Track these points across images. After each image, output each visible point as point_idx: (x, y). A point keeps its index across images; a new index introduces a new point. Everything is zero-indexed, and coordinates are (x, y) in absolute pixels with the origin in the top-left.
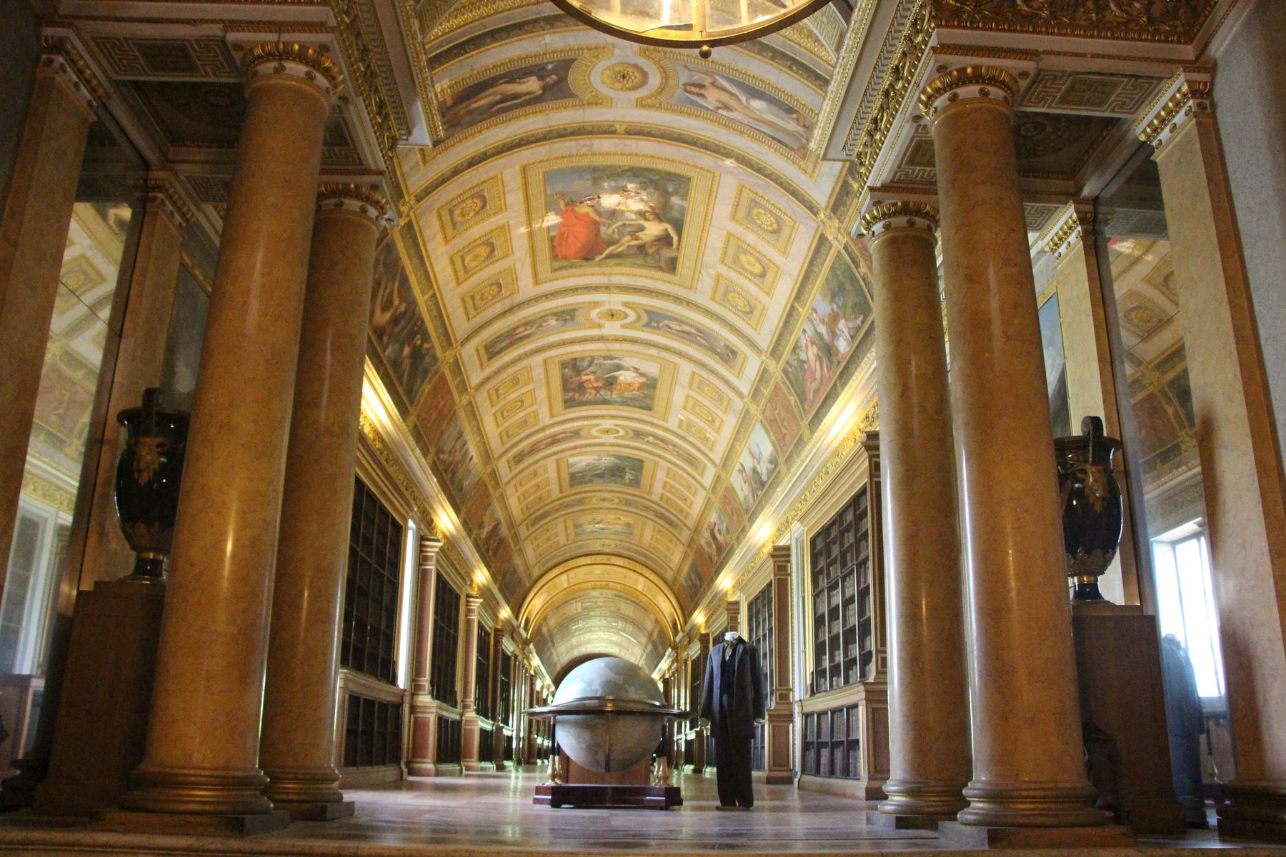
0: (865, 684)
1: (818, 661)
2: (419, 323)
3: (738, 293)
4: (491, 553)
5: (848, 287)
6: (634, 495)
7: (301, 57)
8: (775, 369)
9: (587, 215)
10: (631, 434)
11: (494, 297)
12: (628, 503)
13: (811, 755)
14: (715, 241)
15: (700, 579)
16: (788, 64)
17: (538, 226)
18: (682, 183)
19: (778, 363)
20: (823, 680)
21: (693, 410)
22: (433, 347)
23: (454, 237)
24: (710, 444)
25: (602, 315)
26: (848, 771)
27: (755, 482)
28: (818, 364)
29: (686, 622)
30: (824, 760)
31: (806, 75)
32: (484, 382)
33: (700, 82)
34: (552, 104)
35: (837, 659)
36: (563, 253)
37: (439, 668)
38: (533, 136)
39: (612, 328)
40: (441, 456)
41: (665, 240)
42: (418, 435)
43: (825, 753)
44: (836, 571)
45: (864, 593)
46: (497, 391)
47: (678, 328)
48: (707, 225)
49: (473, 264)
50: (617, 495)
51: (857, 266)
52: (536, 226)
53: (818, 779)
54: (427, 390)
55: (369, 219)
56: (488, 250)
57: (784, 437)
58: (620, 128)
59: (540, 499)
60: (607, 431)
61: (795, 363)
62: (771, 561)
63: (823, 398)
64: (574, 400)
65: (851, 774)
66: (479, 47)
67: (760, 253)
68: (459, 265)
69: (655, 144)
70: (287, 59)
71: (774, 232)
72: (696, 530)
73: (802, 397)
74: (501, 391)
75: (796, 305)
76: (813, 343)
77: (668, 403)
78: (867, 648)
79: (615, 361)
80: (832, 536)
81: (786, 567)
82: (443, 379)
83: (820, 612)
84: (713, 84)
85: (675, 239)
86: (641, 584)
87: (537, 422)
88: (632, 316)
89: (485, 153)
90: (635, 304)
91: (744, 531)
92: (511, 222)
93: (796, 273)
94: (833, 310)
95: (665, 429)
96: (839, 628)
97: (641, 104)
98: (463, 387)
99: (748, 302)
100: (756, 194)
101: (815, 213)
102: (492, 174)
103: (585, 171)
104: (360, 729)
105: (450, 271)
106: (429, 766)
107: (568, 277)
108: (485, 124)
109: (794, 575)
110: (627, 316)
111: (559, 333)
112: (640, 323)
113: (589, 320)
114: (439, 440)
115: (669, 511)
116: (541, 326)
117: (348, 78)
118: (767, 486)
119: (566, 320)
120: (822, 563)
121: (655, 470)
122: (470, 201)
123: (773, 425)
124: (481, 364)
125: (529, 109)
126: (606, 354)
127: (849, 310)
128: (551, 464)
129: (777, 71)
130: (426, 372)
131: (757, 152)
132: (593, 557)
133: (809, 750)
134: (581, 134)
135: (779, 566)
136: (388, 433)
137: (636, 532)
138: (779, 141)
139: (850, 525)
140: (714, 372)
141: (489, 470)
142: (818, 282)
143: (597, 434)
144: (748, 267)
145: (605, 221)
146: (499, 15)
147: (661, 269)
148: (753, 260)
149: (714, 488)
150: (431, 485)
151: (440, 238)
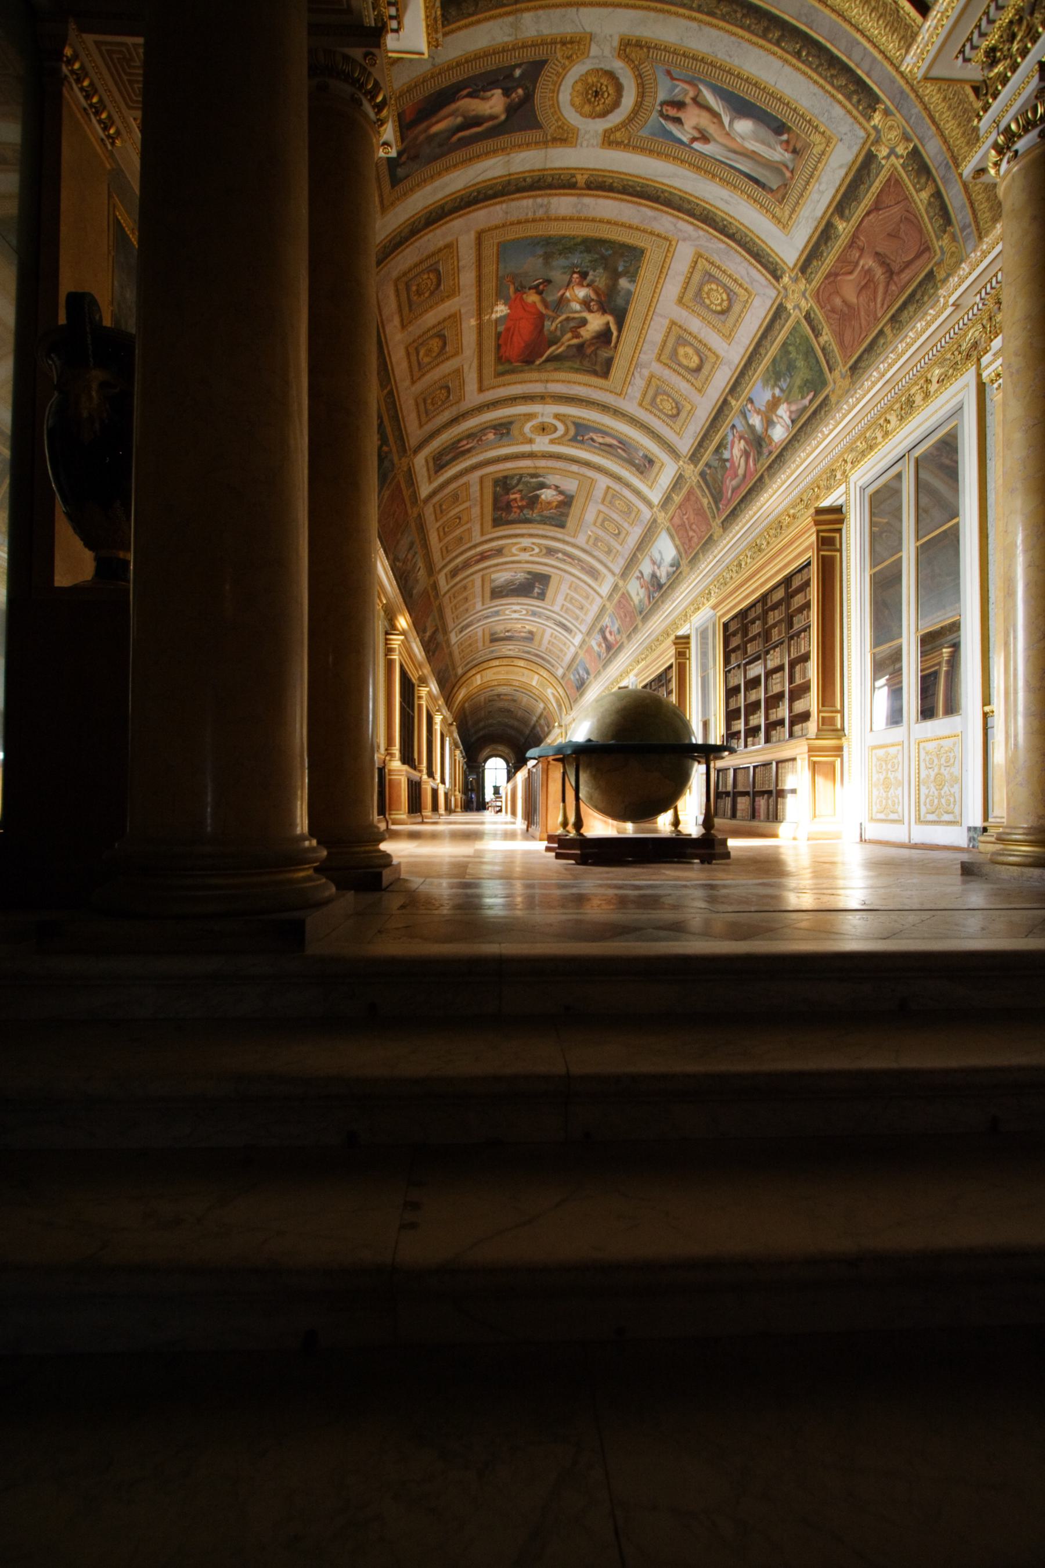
1: (728, 726)
3: (669, 396)
4: (431, 653)
5: (800, 363)
6: (538, 607)
8: (692, 473)
10: (544, 551)
11: (443, 403)
12: (534, 614)
14: (656, 333)
15: (588, 673)
17: (487, 317)
19: (696, 466)
22: (391, 451)
27: (653, 586)
33: (680, 98)
34: (518, 137)
36: (507, 354)
38: (491, 187)
39: (542, 444)
40: (397, 564)
41: (604, 337)
46: (441, 506)
47: (601, 440)
48: (651, 313)
49: (427, 360)
51: (817, 334)
53: (734, 822)
56: (440, 344)
57: (690, 541)
58: (581, 179)
60: (525, 550)
61: (716, 464)
62: (674, 647)
63: (743, 494)
67: (700, 341)
68: (414, 358)
73: (717, 497)
74: (444, 507)
75: (729, 398)
76: (741, 438)
77: (581, 519)
79: (541, 479)
80: (750, 618)
85: (615, 334)
86: (535, 681)
87: (470, 540)
89: (442, 207)
90: (564, 415)
91: (635, 629)
92: (463, 311)
95: (574, 546)
98: (415, 496)
99: (676, 404)
100: (712, 263)
101: (778, 279)
105: (405, 365)
107: (509, 384)
111: (494, 448)
113: (523, 434)
114: (395, 547)
115: (566, 619)
118: (664, 588)
119: (502, 434)
121: (560, 582)
122: (426, 276)
123: (680, 532)
124: (429, 478)
126: (532, 471)
127: (796, 389)
128: (477, 578)
131: (727, 202)
133: (722, 798)
134: (540, 189)
135: (679, 652)
137: (537, 638)
138: (756, 181)
140: (628, 485)
141: (431, 582)
142: (762, 366)
144: (685, 362)
145: (550, 313)
147: (595, 373)
149: (610, 597)
151: (396, 321)
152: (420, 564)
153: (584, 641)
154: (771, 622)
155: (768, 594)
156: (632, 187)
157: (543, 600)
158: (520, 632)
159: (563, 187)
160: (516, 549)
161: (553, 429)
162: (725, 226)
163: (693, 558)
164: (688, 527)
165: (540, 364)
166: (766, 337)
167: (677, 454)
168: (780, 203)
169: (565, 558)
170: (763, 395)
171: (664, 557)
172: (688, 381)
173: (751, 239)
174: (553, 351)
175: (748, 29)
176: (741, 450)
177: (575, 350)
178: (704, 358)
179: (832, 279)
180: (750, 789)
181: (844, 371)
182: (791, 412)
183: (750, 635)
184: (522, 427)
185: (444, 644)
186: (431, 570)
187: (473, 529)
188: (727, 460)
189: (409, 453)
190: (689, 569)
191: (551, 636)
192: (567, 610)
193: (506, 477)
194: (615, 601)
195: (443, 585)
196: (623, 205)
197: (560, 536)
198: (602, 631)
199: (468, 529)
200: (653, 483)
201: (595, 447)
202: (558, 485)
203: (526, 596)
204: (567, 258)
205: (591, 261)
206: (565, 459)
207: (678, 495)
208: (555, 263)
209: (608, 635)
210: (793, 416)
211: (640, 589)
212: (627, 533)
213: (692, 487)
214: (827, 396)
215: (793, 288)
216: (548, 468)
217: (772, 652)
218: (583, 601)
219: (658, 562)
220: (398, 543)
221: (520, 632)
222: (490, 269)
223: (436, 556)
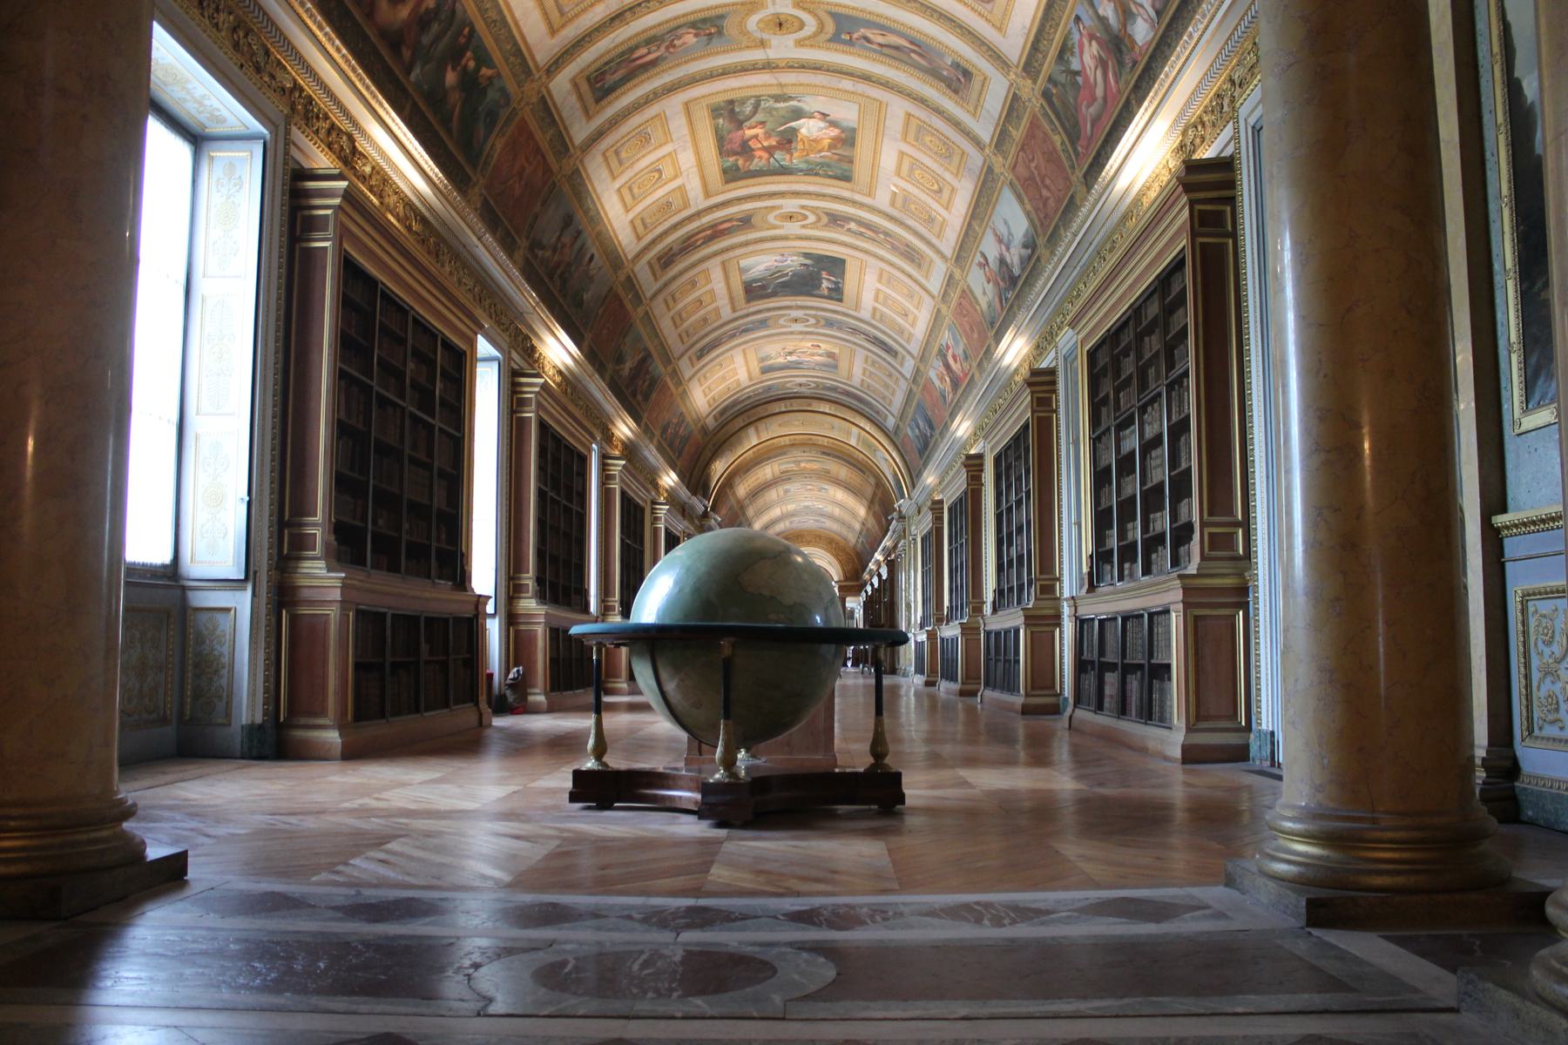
0: (1181, 577)
2: (467, 30)
8: (1030, 92)
10: (825, 219)
12: (830, 324)
13: (1090, 680)
15: (932, 427)
19: (1035, 82)
20: (1108, 567)
21: (910, 178)
22: (499, 75)
24: (936, 229)
25: (764, 24)
26: (1151, 712)
27: (1003, 279)
28: (1099, 73)
29: (914, 487)
30: (1110, 689)
35: (1130, 535)
37: (554, 559)
39: (782, 47)
40: (540, 253)
42: (491, 218)
43: (1111, 679)
44: (1129, 400)
45: (1179, 429)
46: (617, 153)
47: (880, 40)
50: (813, 312)
53: (1102, 720)
54: (499, 147)
57: (1045, 204)
59: (705, 320)
61: (1062, 78)
62: (1028, 391)
64: (738, 168)
65: (1156, 715)
72: (923, 358)
73: (1073, 134)
74: (623, 155)
76: (1092, 37)
77: (874, 166)
78: (1183, 519)
80: (1123, 345)
81: (1051, 398)
83: (1103, 464)
87: (686, 205)
95: (873, 209)
96: (1134, 486)
104: (389, 659)
106: (541, 698)
109: (1062, 411)
110: (802, 25)
111: (702, 57)
115: (884, 333)
118: (1020, 283)
120: (1107, 387)
121: (862, 269)
123: (1028, 188)
130: (492, 117)
132: (788, 402)
133: (1086, 672)
136: (431, 209)
137: (843, 365)
139: (1154, 324)
140: (939, 111)
143: (778, 223)
150: (526, 298)
153: (917, 372)
154: (1147, 355)
155: (1140, 306)
157: (840, 300)
158: (813, 355)
161: (796, 24)
163: (1052, 235)
164: (1039, 183)
167: (1004, 62)
169: (862, 230)
171: (1013, 231)
176: (1095, 57)
180: (1118, 660)
183: (1123, 377)
184: (742, 24)
185: (668, 380)
188: (1077, 73)
189: (537, 76)
190: (1048, 253)
191: (866, 362)
192: (883, 318)
193: (731, 102)
194: (954, 304)
197: (846, 194)
198: (942, 354)
200: (976, 108)
201: (875, 51)
203: (810, 294)
206: (828, 71)
207: (1017, 130)
210: (1158, 5)
211: (985, 283)
212: (953, 190)
213: (1034, 116)
216: (801, 85)
217: (1149, 409)
218: (907, 304)
219: (1005, 240)
220: (536, 217)
221: (813, 355)
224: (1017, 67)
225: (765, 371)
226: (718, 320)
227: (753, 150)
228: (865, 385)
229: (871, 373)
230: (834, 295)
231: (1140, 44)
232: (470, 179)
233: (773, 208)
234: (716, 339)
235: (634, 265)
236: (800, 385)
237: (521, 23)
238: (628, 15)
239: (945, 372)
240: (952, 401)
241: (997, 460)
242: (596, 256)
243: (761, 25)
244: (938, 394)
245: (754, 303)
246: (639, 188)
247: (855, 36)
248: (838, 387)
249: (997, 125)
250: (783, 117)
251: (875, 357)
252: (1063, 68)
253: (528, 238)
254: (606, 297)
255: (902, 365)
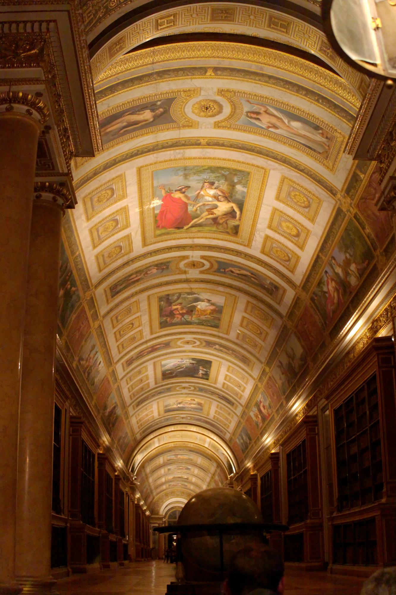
2: (69, 274)
7: (24, 101)
8: (305, 297)
9: (180, 199)
10: (204, 344)
11: (117, 255)
12: (201, 390)
14: (265, 214)
15: (250, 439)
16: (316, 98)
18: (245, 176)
19: (307, 294)
21: (246, 327)
22: (78, 290)
23: (93, 216)
28: (336, 294)
31: (328, 105)
32: (108, 312)
33: (258, 110)
39: (194, 274)
40: (82, 362)
41: (231, 214)
46: (117, 318)
47: (238, 272)
51: (364, 228)
52: (146, 207)
54: (73, 319)
55: (58, 206)
56: (114, 224)
59: (142, 389)
60: (188, 343)
64: (167, 322)
66: (114, 92)
67: (296, 221)
68: (95, 234)
69: (228, 151)
70: (14, 102)
71: (305, 207)
72: (247, 406)
74: (119, 318)
75: (320, 254)
76: (332, 280)
77: (230, 322)
79: (195, 295)
82: (83, 310)
84: (266, 112)
85: (238, 213)
87: (142, 337)
88: (207, 265)
89: (115, 160)
92: (129, 205)
93: (320, 233)
94: (346, 257)
97: (217, 125)
98: (95, 316)
100: (294, 182)
102: (119, 173)
103: (179, 170)
105: (89, 239)
108: (115, 141)
112: (213, 270)
113: (179, 269)
116: (146, 273)
117: (51, 113)
122: (104, 192)
124: (107, 301)
125: (144, 131)
129: (309, 103)
130: (73, 306)
132: (176, 426)
137: (206, 408)
141: (110, 371)
143: (182, 345)
144: (288, 231)
146: (128, 72)
147: (228, 233)
148: (291, 226)
151: (84, 217)
152: (100, 359)
153: (244, 413)
156: (235, 145)
157: (207, 379)
158: (190, 404)
159: (193, 145)
160: (181, 343)
161: (201, 265)
162: (297, 166)
165: (187, 229)
166: (335, 224)
168: (327, 159)
169: (221, 348)
170: (341, 257)
172: (292, 242)
173: (314, 174)
174: (195, 222)
175: (288, 89)
176: (334, 287)
177: (211, 221)
178: (300, 230)
179: (363, 200)
181: (381, 251)
182: (358, 269)
185: (123, 416)
186: (109, 361)
187: (143, 331)
188: (325, 292)
189: (91, 288)
191: (217, 407)
192: (228, 388)
193: (168, 295)
195: (120, 371)
196: (232, 152)
198: (258, 405)
199: (140, 331)
201: (235, 276)
202: (210, 300)
204: (200, 176)
205: (216, 177)
208: (191, 178)
209: (262, 409)
212: (267, 334)
214: (375, 265)
215: (344, 201)
220: (82, 346)
221: (190, 404)
222: (147, 184)
223: (114, 352)
224: (299, 287)
225: (167, 411)
226: (148, 388)
227: (175, 314)
228: (216, 418)
229: (219, 413)
230: (205, 377)
231: (353, 285)
232: (62, 333)
233: (180, 339)
234: (145, 397)
235: (116, 365)
236: (183, 418)
237: (89, 269)
238: (130, 262)
239: (258, 413)
240: (262, 427)
241: (288, 456)
242: (102, 363)
243: (185, 265)
244: (254, 424)
245: (165, 381)
246: (123, 331)
247: (227, 270)
248: (202, 419)
249: (290, 308)
250: (190, 301)
251: (223, 406)
252: (320, 290)
253: (78, 356)
254: (103, 379)
255: (236, 409)
